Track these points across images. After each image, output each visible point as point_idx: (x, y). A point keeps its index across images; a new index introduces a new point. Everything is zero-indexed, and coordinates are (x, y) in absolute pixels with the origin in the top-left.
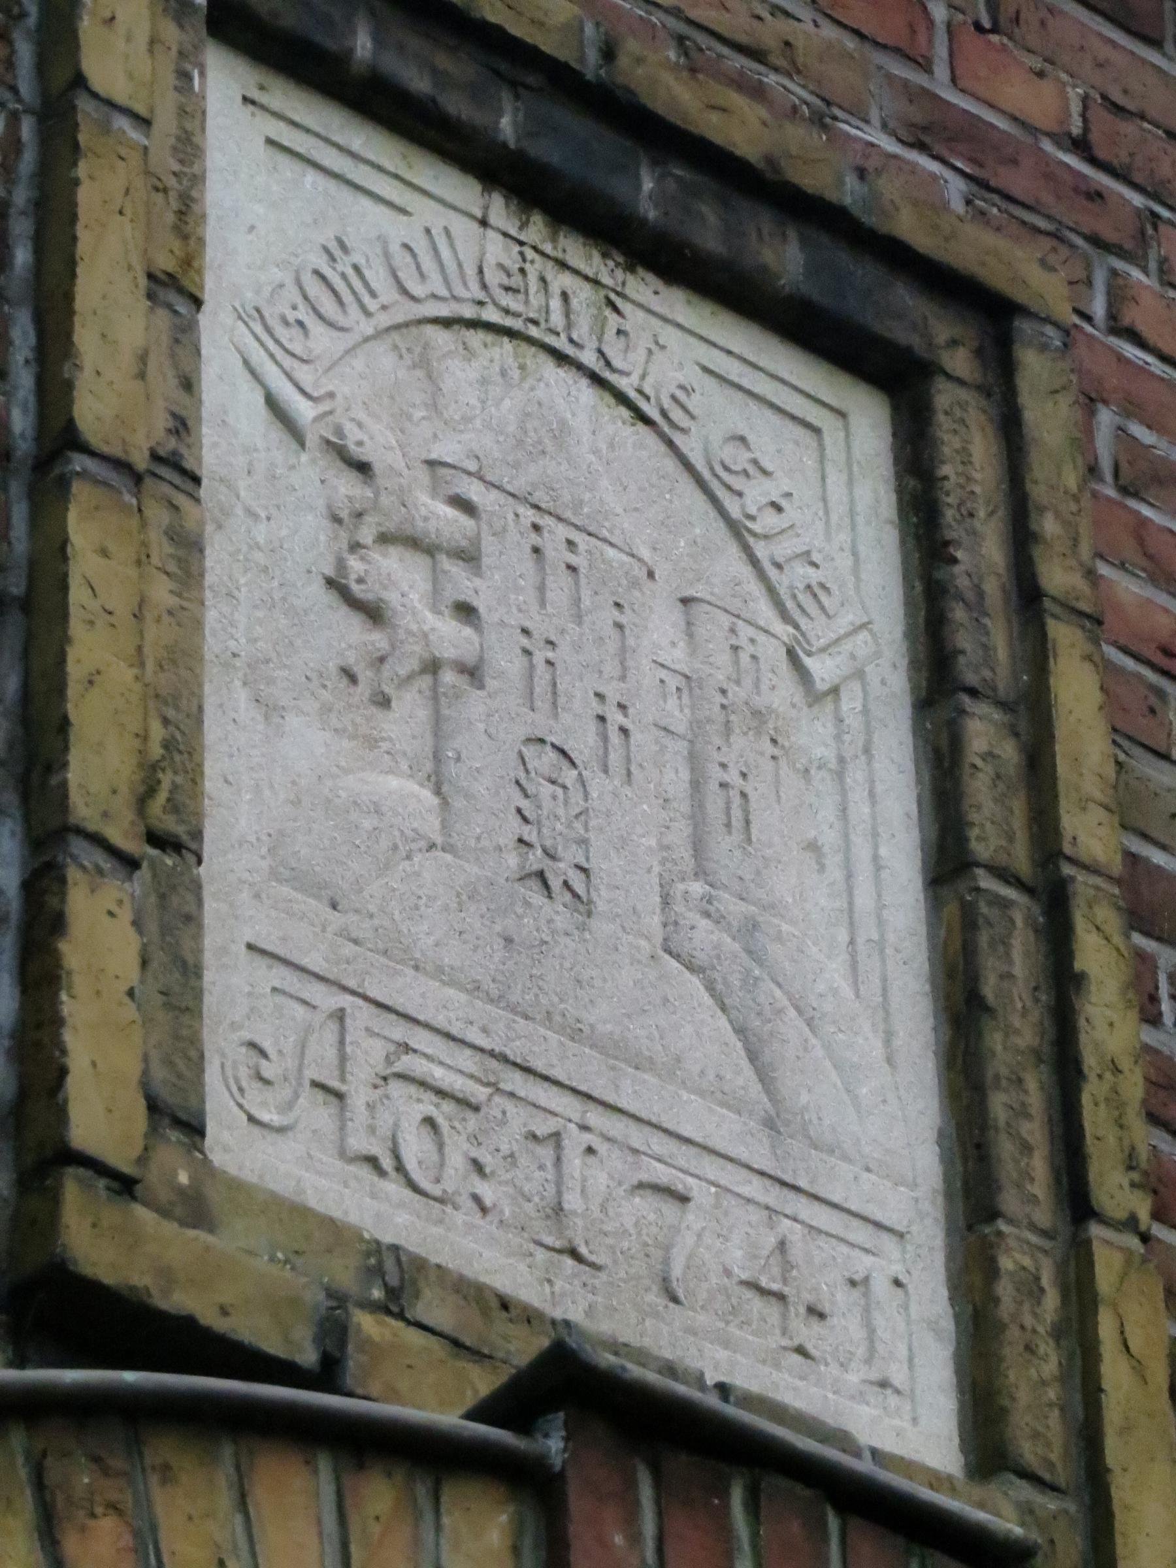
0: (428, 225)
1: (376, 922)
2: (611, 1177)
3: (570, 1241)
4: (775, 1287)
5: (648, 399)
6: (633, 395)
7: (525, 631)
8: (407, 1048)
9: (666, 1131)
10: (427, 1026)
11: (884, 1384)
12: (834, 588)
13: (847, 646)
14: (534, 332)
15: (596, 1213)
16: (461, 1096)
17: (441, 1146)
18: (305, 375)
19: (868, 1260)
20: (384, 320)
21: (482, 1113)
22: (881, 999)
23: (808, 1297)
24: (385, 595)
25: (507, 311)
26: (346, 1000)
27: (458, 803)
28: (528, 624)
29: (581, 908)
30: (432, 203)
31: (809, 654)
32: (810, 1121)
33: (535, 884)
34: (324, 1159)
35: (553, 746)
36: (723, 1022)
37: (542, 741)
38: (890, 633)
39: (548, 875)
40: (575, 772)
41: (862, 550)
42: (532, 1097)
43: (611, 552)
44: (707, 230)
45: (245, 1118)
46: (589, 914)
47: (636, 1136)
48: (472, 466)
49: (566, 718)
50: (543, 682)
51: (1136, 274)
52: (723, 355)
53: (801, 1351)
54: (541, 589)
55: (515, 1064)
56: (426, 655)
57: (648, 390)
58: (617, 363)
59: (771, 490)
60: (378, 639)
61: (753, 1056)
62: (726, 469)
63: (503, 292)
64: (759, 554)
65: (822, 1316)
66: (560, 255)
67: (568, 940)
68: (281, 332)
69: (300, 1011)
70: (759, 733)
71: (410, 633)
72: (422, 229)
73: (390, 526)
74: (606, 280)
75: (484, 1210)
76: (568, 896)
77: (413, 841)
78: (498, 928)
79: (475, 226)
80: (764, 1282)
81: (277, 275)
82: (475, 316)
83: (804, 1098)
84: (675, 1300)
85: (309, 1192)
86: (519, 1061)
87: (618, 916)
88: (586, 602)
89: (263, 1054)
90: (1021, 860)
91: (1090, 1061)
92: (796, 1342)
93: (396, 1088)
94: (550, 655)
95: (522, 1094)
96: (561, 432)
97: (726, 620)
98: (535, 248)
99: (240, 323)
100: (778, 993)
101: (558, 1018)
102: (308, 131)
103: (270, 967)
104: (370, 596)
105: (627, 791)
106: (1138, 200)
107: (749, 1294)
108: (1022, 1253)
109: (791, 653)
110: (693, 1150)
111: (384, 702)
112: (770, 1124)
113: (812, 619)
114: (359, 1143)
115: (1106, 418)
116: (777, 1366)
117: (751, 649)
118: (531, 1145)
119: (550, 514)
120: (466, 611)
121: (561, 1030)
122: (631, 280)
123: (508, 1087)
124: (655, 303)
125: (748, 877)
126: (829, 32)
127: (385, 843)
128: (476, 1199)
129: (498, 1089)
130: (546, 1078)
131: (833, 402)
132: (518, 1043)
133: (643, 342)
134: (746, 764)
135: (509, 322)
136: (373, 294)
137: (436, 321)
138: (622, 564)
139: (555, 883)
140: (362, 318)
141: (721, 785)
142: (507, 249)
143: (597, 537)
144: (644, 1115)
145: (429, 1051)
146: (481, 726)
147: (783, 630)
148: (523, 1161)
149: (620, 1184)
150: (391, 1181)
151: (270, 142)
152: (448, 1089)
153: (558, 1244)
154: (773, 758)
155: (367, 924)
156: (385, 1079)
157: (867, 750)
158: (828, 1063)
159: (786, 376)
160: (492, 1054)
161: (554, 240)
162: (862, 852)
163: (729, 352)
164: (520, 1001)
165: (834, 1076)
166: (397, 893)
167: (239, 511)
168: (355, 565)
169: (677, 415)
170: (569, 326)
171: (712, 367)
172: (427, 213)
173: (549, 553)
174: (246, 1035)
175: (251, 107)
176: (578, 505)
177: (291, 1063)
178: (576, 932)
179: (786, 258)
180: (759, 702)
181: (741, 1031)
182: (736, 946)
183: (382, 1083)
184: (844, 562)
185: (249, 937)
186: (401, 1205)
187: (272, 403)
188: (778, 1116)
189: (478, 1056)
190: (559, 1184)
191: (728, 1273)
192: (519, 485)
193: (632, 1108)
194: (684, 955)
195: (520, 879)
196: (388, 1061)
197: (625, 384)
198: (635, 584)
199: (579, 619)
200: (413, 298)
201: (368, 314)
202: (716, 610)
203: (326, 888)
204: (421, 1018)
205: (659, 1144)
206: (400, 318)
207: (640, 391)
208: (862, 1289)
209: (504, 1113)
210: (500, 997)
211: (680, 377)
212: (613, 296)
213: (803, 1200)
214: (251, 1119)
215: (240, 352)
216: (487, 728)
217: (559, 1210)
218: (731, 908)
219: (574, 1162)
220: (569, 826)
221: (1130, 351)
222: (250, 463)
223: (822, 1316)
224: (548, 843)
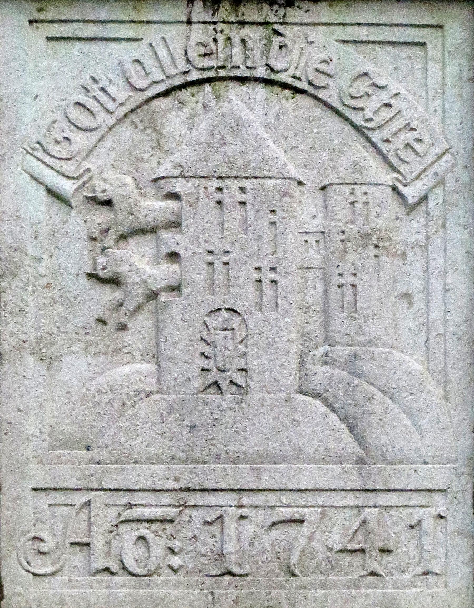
0: (150, 42)
1: (110, 448)
2: (257, 525)
3: (227, 569)
4: (357, 547)
5: (300, 79)
6: (289, 81)
7: (210, 252)
8: (130, 506)
9: (291, 490)
10: (141, 490)
11: (427, 573)
12: (426, 137)
13: (434, 169)
14: (222, 73)
15: (247, 547)
16: (161, 518)
17: (149, 548)
18: (69, 168)
19: (422, 511)
20: (123, 111)
21: (176, 522)
22: (443, 365)
23: (380, 544)
24: (119, 270)
25: (203, 69)
26: (90, 496)
27: (164, 364)
28: (211, 248)
29: (242, 391)
30: (156, 26)
31: (405, 185)
32: (387, 451)
33: (213, 389)
34: (79, 579)
35: (226, 309)
36: (333, 417)
37: (219, 309)
38: (464, 149)
39: (219, 382)
40: (241, 318)
41: (447, 106)
42: (207, 502)
43: (269, 182)
45: (31, 576)
46: (247, 392)
47: (272, 499)
48: (177, 172)
49: (235, 291)
50: (221, 277)
52: (357, 28)
53: (373, 574)
54: (222, 224)
55: (195, 490)
56: (147, 292)
57: (298, 74)
58: (278, 65)
59: (384, 97)
61: (351, 430)
62: (353, 97)
63: (202, 58)
64: (374, 139)
65: (389, 551)
66: (240, 18)
67: (232, 413)
68: (54, 149)
69: (65, 510)
70: (365, 246)
71: (134, 284)
72: (148, 45)
73: (124, 229)
74: (273, 19)
75: (175, 571)
76: (234, 388)
77: (136, 396)
78: (186, 423)
79: (184, 27)
80: (350, 547)
81: (51, 117)
82: (183, 81)
83: (384, 439)
84: (294, 575)
85: (67, 599)
86: (197, 488)
87: (264, 386)
88: (251, 218)
89: (42, 540)
92: (369, 571)
93: (123, 529)
94: (225, 259)
95: (201, 503)
96: (237, 127)
97: (346, 190)
98: (224, 22)
99: (29, 157)
100: (371, 388)
101: (223, 456)
102: (72, 21)
103: (47, 495)
104: (111, 274)
105: (275, 315)
107: (342, 555)
109: (394, 189)
110: (309, 494)
112: (361, 461)
113: (408, 163)
114: (100, 563)
116: (357, 587)
117: (364, 199)
118: (206, 528)
119: (229, 177)
120: (174, 256)
121: (227, 461)
122: (290, 11)
123: (192, 503)
124: (306, 19)
125: (352, 332)
127: (117, 404)
128: (170, 567)
129: (186, 506)
130: (215, 490)
131: (434, 22)
132: (197, 479)
133: (301, 43)
134: (356, 269)
135: (206, 75)
136: (114, 99)
137: (158, 96)
138: (275, 186)
139: (224, 385)
140: (108, 116)
141: (339, 286)
142: (205, 32)
143: (260, 178)
144: (276, 487)
145: (143, 502)
146: (179, 317)
147: (389, 178)
148: (202, 538)
149: (263, 527)
150: (119, 576)
151: (49, 39)
152: (153, 518)
153: (219, 573)
154: (376, 256)
155: (105, 451)
156: (117, 526)
157: (443, 226)
158: (403, 415)
159: (399, 21)
160: (181, 490)
161: (236, 11)
162: (436, 284)
163: (359, 24)
164: (200, 456)
165: (407, 421)
166: (123, 428)
167: (28, 261)
168: (101, 260)
169: (321, 80)
170: (246, 57)
171: (347, 39)
172: (152, 34)
173: (227, 202)
174: (31, 535)
175: (35, 25)
176: (245, 168)
177: (60, 539)
178: (236, 406)
180: (367, 229)
181: (344, 419)
182: (345, 373)
183: (115, 529)
184: (434, 121)
185: (33, 484)
186: (124, 585)
187: (50, 191)
188: (367, 455)
189: (173, 494)
190: (222, 541)
191: (330, 549)
192: (208, 169)
193: (268, 487)
194: (310, 391)
195: (203, 391)
196: (119, 515)
197: (284, 78)
198: (286, 194)
199: (246, 231)
200: (141, 90)
201: (111, 113)
202: (340, 186)
203: (81, 442)
204: (136, 488)
205: (285, 498)
206: (133, 106)
207: (294, 77)
208: (418, 528)
209: (190, 517)
210: (187, 458)
211: (323, 56)
212: (276, 27)
213: (381, 494)
214: (35, 575)
215: (28, 173)
217: (221, 555)
218: (341, 353)
219: (231, 526)
220: (236, 348)
222: (36, 232)
223: (389, 551)
224: (220, 365)
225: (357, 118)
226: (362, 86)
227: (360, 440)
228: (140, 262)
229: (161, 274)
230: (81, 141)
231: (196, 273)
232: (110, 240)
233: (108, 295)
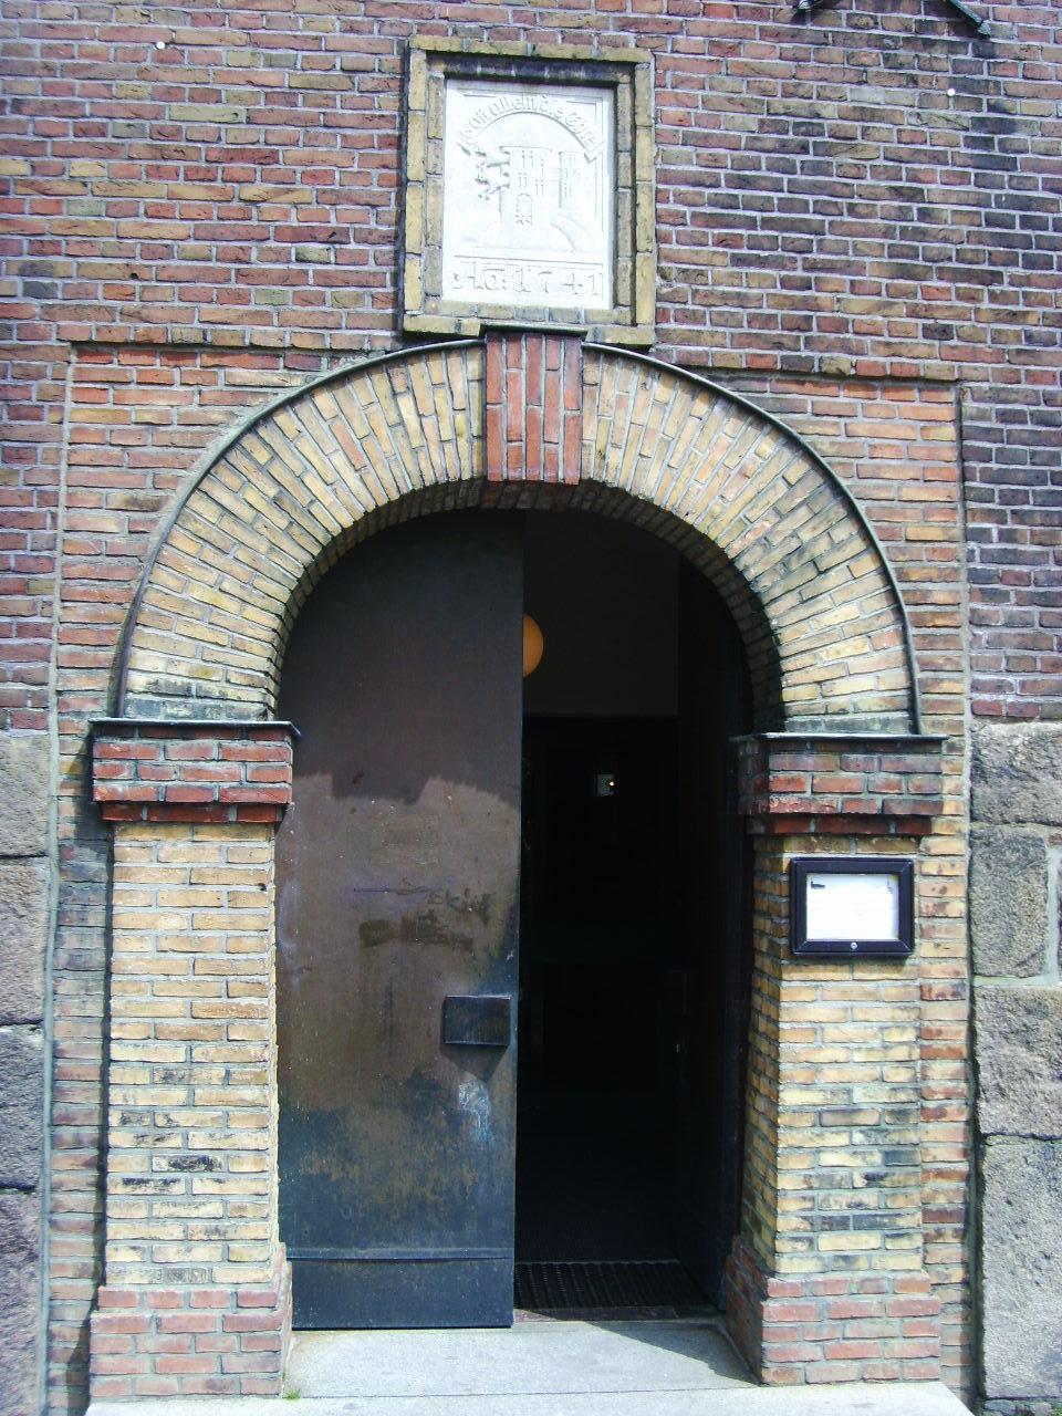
18: (470, 141)
44: (562, 75)
51: (679, 37)
59: (581, 122)
60: (486, 187)
90: (629, 183)
91: (638, 221)
106: (680, 19)
108: (625, 262)
111: (487, 199)
115: (669, 74)
120: (506, 174)
126: (600, 14)
179: (581, 74)
216: (510, 196)
221: (676, 55)
225: (572, 129)
226: (574, 117)
227: (572, 243)
228: (494, 176)
229: (503, 180)
230: (475, 132)
231: (514, 180)
232: (484, 167)
233: (484, 187)
